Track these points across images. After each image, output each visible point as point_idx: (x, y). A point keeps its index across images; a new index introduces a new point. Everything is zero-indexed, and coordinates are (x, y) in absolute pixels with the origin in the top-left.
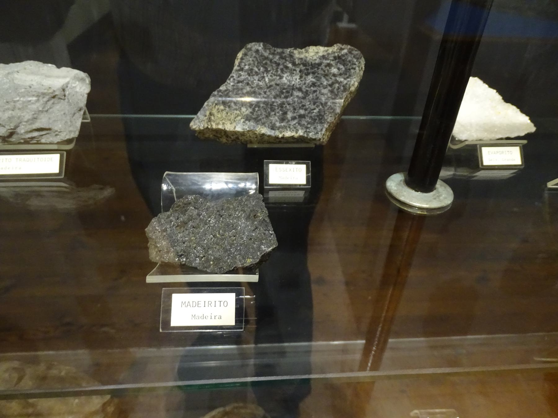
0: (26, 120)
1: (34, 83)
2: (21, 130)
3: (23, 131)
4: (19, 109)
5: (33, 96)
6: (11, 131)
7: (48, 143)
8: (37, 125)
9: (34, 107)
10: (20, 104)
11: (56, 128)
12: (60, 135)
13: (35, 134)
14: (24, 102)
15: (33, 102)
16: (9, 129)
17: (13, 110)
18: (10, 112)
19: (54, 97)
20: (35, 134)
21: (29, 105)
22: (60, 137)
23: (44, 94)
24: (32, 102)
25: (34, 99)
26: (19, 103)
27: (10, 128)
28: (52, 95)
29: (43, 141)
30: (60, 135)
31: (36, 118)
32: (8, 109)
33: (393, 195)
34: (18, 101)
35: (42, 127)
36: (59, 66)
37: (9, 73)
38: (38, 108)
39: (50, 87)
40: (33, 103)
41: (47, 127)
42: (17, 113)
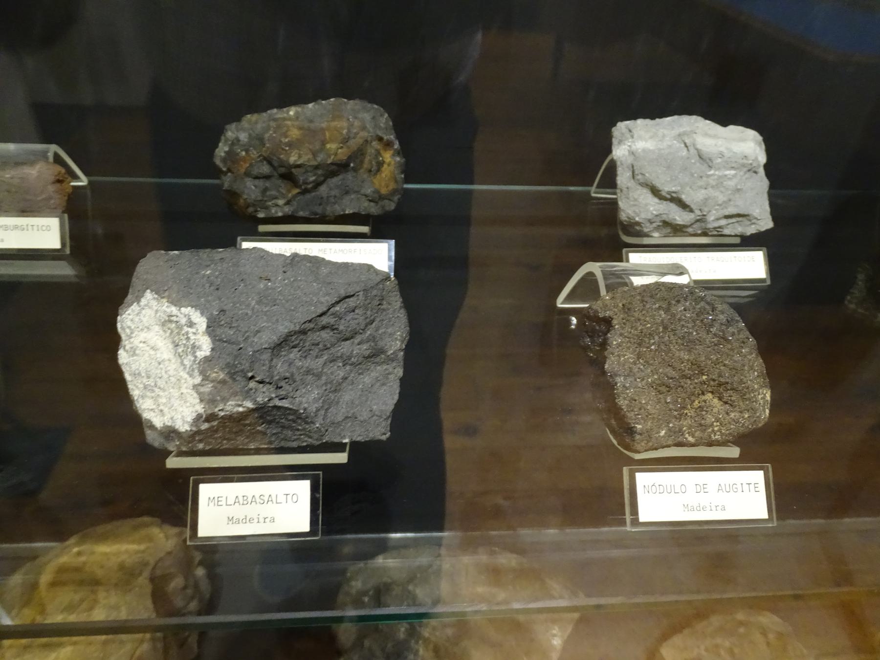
0: (720, 202)
1: (722, 149)
2: (711, 218)
3: (712, 218)
4: (713, 187)
5: (733, 168)
6: (698, 218)
7: (733, 234)
8: (731, 210)
9: (731, 184)
10: (714, 180)
11: (755, 214)
12: (758, 224)
13: (723, 222)
14: (720, 177)
15: (731, 177)
16: (699, 216)
17: (706, 189)
18: (703, 191)
19: (749, 171)
20: (723, 222)
21: (725, 181)
22: (756, 227)
23: (743, 165)
24: (729, 176)
25: (733, 172)
26: (712, 178)
27: (701, 214)
28: (750, 167)
29: (726, 232)
30: (758, 224)
31: (730, 200)
32: (701, 187)
34: (712, 175)
35: (741, 212)
36: (724, 123)
37: (679, 135)
38: (736, 185)
39: (746, 155)
40: (730, 179)
41: (746, 213)
42: (711, 192)
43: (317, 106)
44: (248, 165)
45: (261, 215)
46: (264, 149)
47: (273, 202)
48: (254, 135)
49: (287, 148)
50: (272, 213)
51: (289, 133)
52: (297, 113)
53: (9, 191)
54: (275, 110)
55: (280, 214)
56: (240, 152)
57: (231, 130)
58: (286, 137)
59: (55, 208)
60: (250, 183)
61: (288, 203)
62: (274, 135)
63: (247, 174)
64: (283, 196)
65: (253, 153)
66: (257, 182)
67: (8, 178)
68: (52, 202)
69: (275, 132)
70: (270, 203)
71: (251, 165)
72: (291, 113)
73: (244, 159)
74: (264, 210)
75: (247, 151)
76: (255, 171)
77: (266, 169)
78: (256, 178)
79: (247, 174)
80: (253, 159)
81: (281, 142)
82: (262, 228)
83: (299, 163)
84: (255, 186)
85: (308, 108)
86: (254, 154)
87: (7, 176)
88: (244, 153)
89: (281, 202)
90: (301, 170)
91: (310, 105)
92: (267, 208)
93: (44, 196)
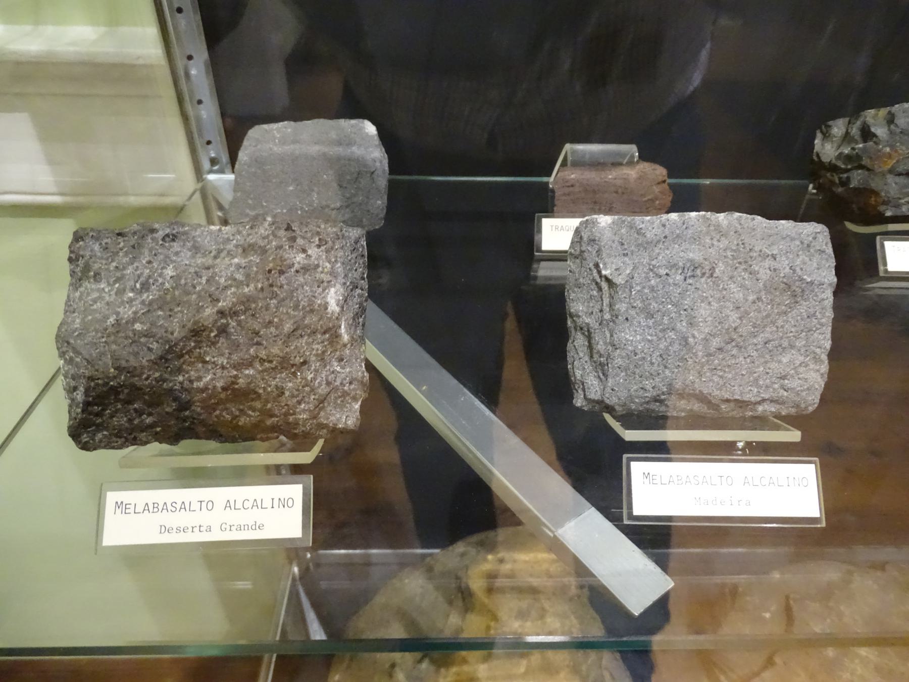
44: (895, 161)
45: (888, 214)
48: (898, 130)
50: (903, 212)
53: (616, 192)
59: (660, 209)
60: (890, 179)
63: (891, 171)
65: (901, 149)
66: (897, 179)
67: (611, 179)
68: (657, 202)
71: (898, 161)
73: (890, 156)
75: (892, 147)
78: (900, 174)
79: (891, 171)
80: (900, 155)
82: (892, 227)
84: (896, 183)
87: (610, 177)
88: (888, 149)
92: (898, 206)
93: (650, 197)
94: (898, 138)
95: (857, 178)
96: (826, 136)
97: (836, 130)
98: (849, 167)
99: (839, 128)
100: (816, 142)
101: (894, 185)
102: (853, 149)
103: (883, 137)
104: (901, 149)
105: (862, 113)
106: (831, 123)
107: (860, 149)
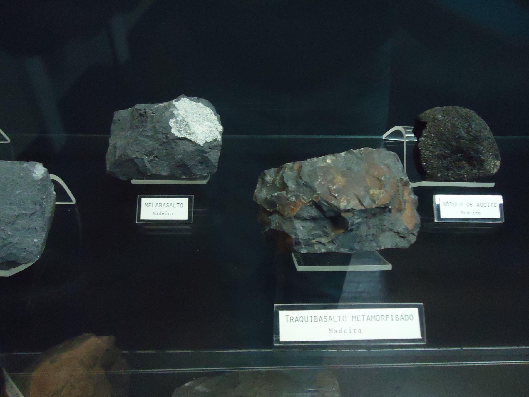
33: (420, 216)
43: (349, 155)
46: (315, 196)
47: (317, 240)
48: (302, 182)
49: (336, 195)
51: (336, 181)
52: (333, 161)
54: (315, 159)
55: (323, 251)
56: (290, 198)
57: (269, 174)
58: (334, 184)
60: (299, 225)
61: (332, 242)
62: (323, 183)
63: (298, 217)
64: (326, 235)
65: (303, 199)
66: (305, 224)
69: (322, 180)
70: (314, 241)
72: (328, 161)
74: (307, 247)
75: (297, 197)
76: (305, 215)
77: (314, 212)
81: (329, 189)
83: (349, 208)
84: (303, 227)
85: (341, 156)
86: (305, 199)
89: (324, 240)
90: (350, 215)
91: (343, 154)
94: (301, 189)
95: (275, 222)
96: (264, 183)
97: (269, 178)
98: (272, 210)
99: (270, 176)
100: (258, 186)
101: (301, 228)
102: (272, 196)
103: (292, 187)
104: (303, 199)
105: (284, 165)
106: (266, 171)
107: (275, 196)
